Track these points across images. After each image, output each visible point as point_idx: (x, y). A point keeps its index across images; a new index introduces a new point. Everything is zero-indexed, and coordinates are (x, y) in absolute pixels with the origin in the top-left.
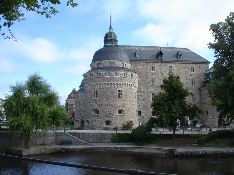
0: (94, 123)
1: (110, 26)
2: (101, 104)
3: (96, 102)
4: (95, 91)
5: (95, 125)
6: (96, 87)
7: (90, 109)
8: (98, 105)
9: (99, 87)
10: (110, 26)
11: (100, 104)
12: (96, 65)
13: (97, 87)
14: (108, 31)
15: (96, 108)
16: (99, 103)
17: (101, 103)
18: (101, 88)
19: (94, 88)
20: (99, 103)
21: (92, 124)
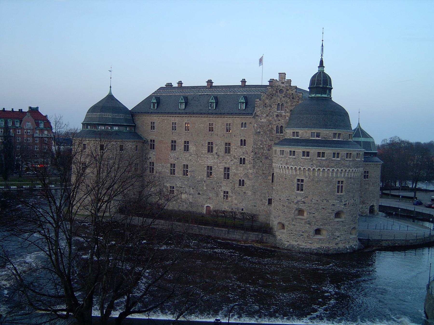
0: (337, 234)
1: (322, 62)
2: (347, 203)
3: (341, 200)
4: (339, 182)
5: (338, 237)
6: (343, 176)
7: (330, 211)
8: (345, 205)
9: (346, 176)
10: (322, 62)
11: (346, 203)
12: (332, 135)
13: (344, 175)
14: (316, 70)
15: (340, 209)
16: (345, 201)
17: (348, 201)
18: (348, 178)
19: (339, 176)
20: (345, 201)
21: (333, 235)
